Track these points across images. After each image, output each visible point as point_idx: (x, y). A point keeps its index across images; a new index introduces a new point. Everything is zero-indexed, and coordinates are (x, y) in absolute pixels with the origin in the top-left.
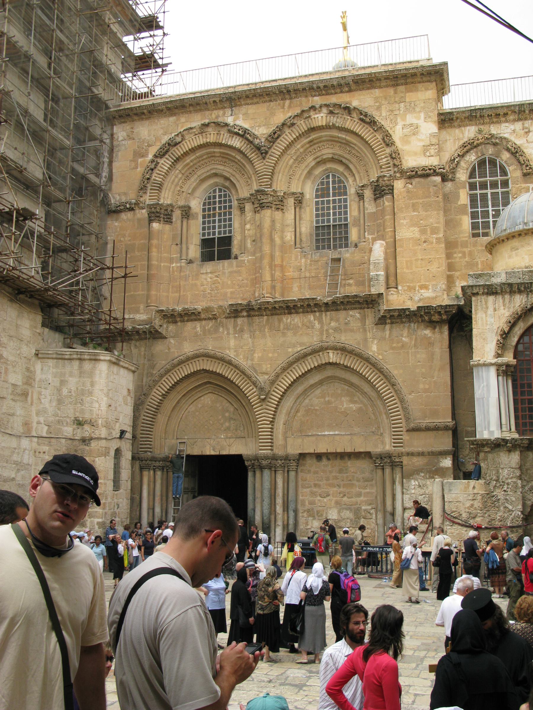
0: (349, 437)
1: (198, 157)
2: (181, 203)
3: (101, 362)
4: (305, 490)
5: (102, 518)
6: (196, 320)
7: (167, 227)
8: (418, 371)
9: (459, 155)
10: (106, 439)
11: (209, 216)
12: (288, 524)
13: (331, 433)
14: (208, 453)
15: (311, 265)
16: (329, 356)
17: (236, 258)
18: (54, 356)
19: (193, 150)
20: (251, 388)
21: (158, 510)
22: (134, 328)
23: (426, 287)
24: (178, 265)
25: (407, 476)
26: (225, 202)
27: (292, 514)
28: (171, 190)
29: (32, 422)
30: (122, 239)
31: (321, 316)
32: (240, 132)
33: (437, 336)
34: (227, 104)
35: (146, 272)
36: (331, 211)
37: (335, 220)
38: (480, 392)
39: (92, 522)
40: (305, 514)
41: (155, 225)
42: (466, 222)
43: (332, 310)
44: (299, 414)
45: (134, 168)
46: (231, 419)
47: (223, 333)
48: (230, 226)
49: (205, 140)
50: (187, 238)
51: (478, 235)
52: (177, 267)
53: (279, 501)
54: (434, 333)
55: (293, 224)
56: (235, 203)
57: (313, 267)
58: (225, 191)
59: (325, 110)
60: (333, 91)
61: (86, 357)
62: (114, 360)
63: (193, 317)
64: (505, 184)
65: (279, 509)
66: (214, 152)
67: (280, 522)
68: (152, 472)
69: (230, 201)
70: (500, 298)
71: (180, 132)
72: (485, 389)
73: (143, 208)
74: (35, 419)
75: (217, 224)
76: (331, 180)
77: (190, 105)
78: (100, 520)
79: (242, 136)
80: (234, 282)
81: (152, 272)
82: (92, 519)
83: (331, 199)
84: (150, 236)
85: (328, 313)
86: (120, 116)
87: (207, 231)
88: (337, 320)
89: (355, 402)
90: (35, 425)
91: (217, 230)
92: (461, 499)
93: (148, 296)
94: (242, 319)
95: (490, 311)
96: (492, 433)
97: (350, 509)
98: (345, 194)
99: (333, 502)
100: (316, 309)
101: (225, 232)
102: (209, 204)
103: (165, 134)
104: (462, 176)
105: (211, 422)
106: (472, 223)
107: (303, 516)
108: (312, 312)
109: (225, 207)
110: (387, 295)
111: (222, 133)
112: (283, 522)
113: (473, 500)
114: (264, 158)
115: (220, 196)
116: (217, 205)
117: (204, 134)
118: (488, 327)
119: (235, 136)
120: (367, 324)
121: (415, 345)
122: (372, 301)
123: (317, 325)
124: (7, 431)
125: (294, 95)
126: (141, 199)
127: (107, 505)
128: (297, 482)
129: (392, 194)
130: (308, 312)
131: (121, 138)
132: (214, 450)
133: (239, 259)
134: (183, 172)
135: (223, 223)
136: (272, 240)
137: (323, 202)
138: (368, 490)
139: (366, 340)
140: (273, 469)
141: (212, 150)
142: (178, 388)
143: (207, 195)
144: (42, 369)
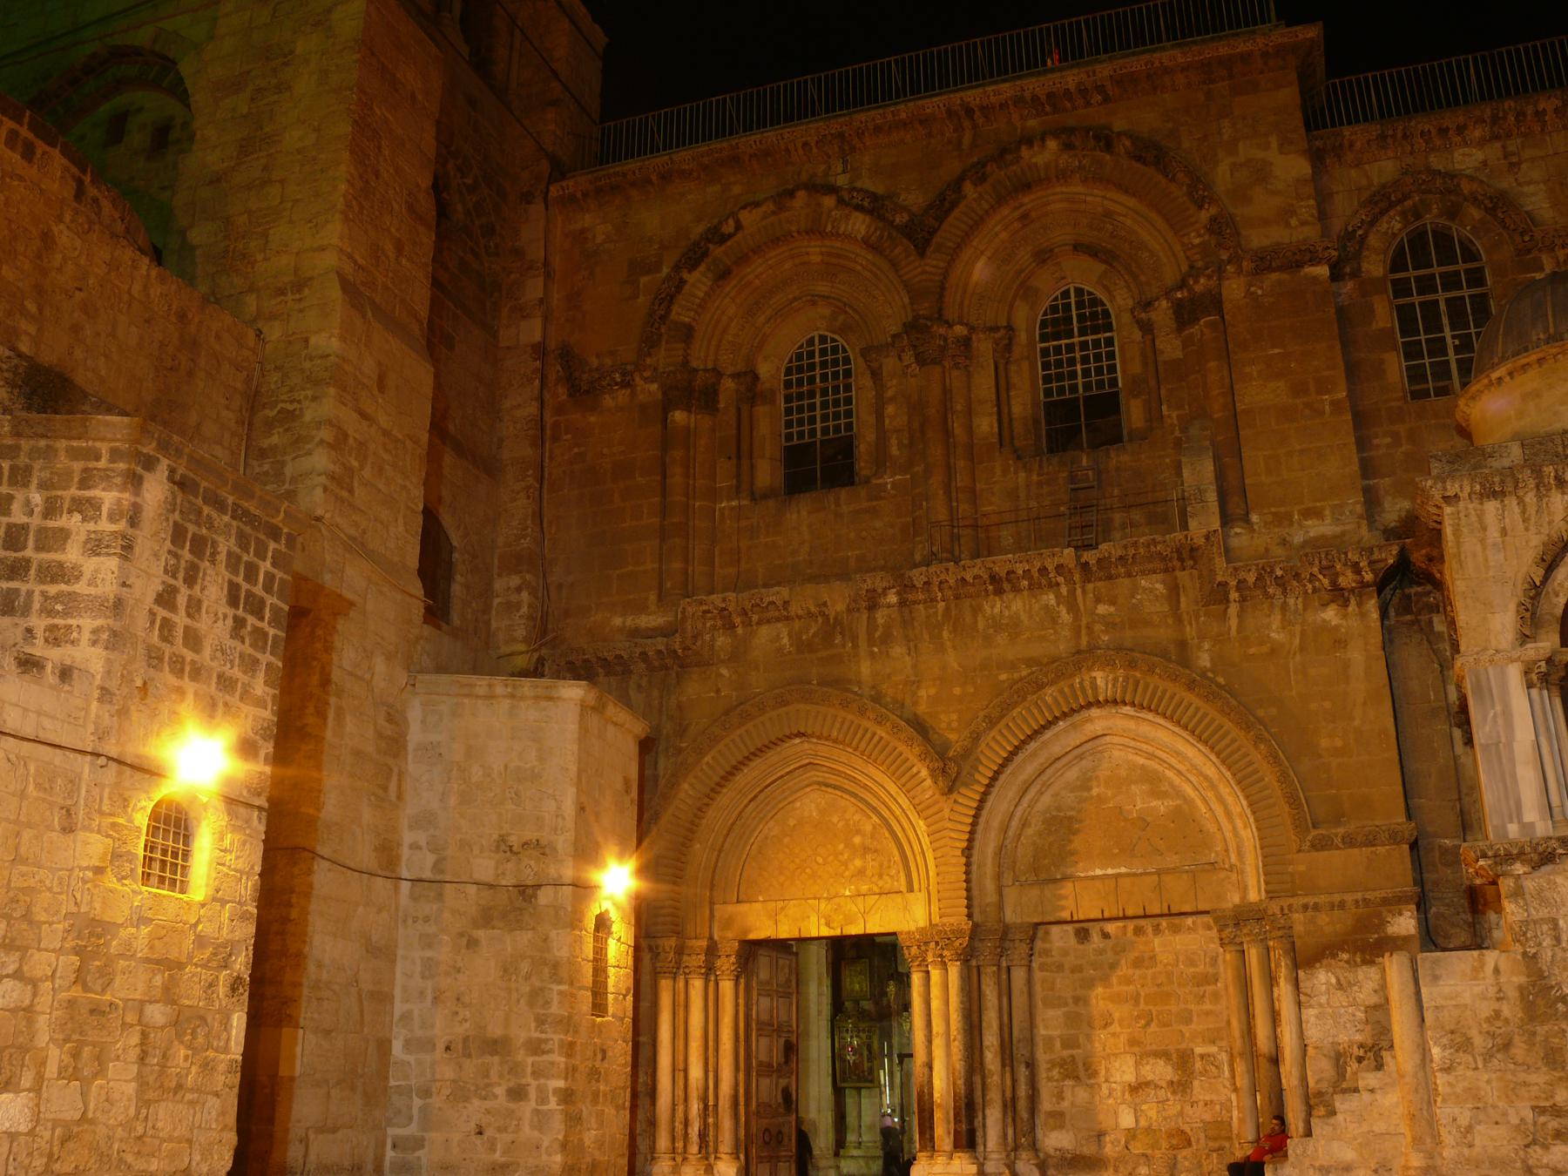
0: (1155, 877)
4: (1051, 1013)
5: (566, 1079)
6: (778, 620)
8: (1313, 706)
9: (1362, 221)
11: (800, 396)
12: (1014, 1098)
13: (1110, 871)
14: (814, 934)
15: (1040, 484)
16: (1094, 686)
17: (867, 481)
20: (915, 770)
21: (696, 1072)
23: (1317, 514)
25: (1303, 959)
26: (835, 363)
27: (1022, 1072)
29: (399, 845)
30: (605, 451)
31: (1072, 592)
32: (866, 204)
33: (1354, 623)
36: (1079, 367)
37: (1087, 386)
38: (1487, 728)
39: (541, 1090)
40: (1055, 1073)
41: (679, 416)
42: (1395, 367)
43: (1100, 579)
44: (1029, 831)
46: (866, 850)
47: (844, 646)
48: (849, 414)
50: (751, 444)
51: (1425, 394)
52: (732, 509)
53: (991, 1039)
54: (1345, 616)
55: (994, 397)
56: (857, 364)
57: (1046, 489)
58: (833, 340)
59: (1052, 144)
60: (1069, 105)
63: (772, 613)
64: (1476, 278)
65: (991, 1059)
67: (994, 1095)
68: (681, 984)
69: (847, 360)
70: (1512, 502)
72: (1500, 721)
74: (408, 837)
75: (818, 412)
76: (1073, 300)
78: (561, 1084)
79: (870, 212)
80: (864, 534)
82: (542, 1081)
83: (1076, 340)
85: (1090, 586)
87: (795, 430)
88: (1113, 602)
89: (1162, 795)
90: (405, 852)
91: (819, 426)
92: (1467, 998)
94: (885, 611)
95: (1493, 533)
96: (1527, 827)
97: (1165, 1055)
98: (1109, 328)
99: (1123, 1039)
100: (1061, 579)
101: (837, 429)
102: (800, 369)
104: (1374, 266)
105: (820, 860)
106: (1408, 368)
107: (1049, 1079)
108: (1050, 585)
109: (836, 375)
110: (1226, 537)
112: (1004, 1092)
113: (1498, 999)
114: (922, 254)
115: (823, 352)
116: (818, 371)
118: (1491, 573)
119: (857, 214)
120: (1183, 605)
121: (1302, 649)
122: (1192, 550)
123: (1065, 616)
125: (980, 121)
127: (578, 1048)
128: (1030, 994)
129: (1220, 312)
130: (1040, 587)
131: (600, 238)
132: (828, 924)
133: (874, 481)
135: (831, 410)
136: (947, 433)
137: (1058, 350)
138: (1207, 1006)
139: (1182, 645)
140: (974, 963)
142: (740, 779)
143: (794, 350)
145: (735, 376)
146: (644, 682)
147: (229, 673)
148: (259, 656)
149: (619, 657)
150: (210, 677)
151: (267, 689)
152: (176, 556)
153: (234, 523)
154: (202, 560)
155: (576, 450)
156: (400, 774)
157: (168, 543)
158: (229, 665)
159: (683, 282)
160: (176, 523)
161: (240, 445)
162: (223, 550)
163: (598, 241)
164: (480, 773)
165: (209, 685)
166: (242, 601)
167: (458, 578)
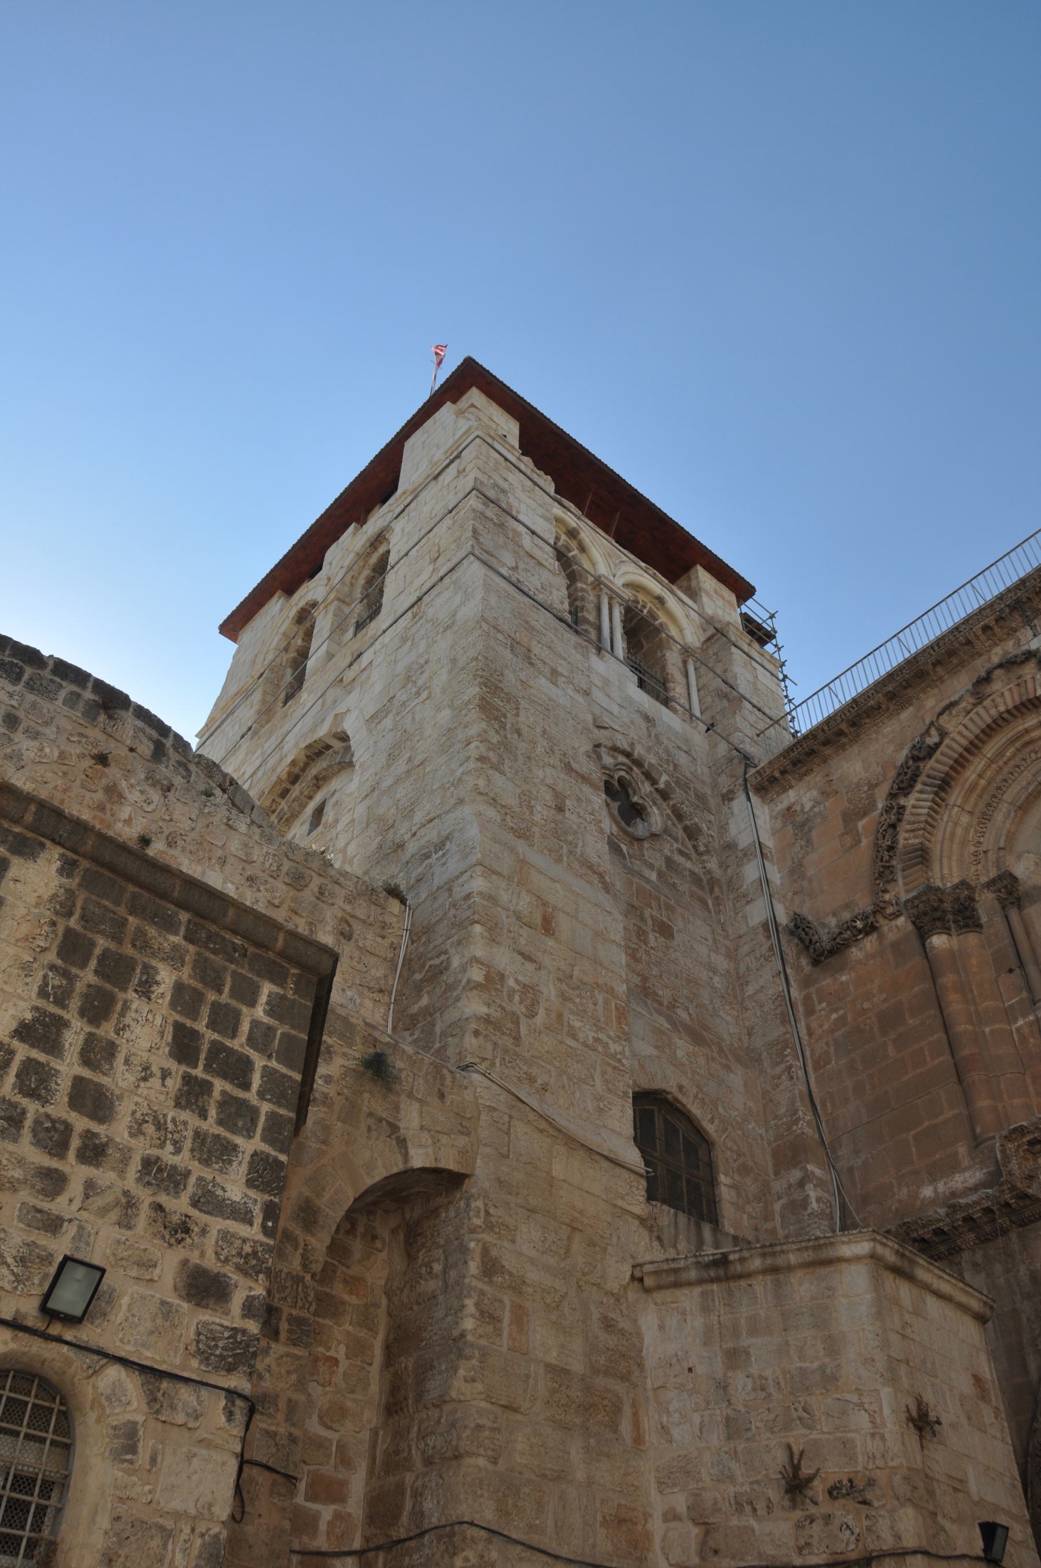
1: (992, 761)
2: (992, 875)
3: (844, 1266)
7: (972, 939)
10: (925, 1553)
18: (693, 1274)
19: (973, 748)
22: (954, 1208)
24: (1031, 1018)
28: (954, 857)
29: (647, 1516)
30: (866, 1005)
34: (1016, 620)
35: (946, 1057)
41: (938, 941)
45: (852, 847)
49: (993, 712)
61: (793, 1258)
62: (891, 1258)
66: (1027, 731)
71: (932, 724)
73: (896, 915)
74: (657, 1503)
77: (937, 663)
81: (965, 1052)
84: (932, 967)
86: (795, 763)
93: (972, 1119)
103: (901, 747)
111: (1028, 677)
117: (987, 703)
124: (535, 1540)
126: (887, 897)
131: (808, 806)
134: (968, 808)
141: (1021, 728)
144: (661, 1327)
145: (990, 884)
146: (979, 1257)
147: (167, 1155)
148: (238, 1140)
149: (938, 1232)
150: (125, 1161)
151: (252, 1193)
152: (65, 974)
153: (192, 948)
154: (124, 989)
155: (834, 1016)
156: (634, 1405)
157: (52, 957)
158: (169, 1148)
159: (903, 808)
160: (69, 932)
161: (386, 1014)
162: (166, 977)
163: (807, 809)
164: (749, 1387)
165: (122, 1173)
166: (203, 1056)
167: (722, 1178)
